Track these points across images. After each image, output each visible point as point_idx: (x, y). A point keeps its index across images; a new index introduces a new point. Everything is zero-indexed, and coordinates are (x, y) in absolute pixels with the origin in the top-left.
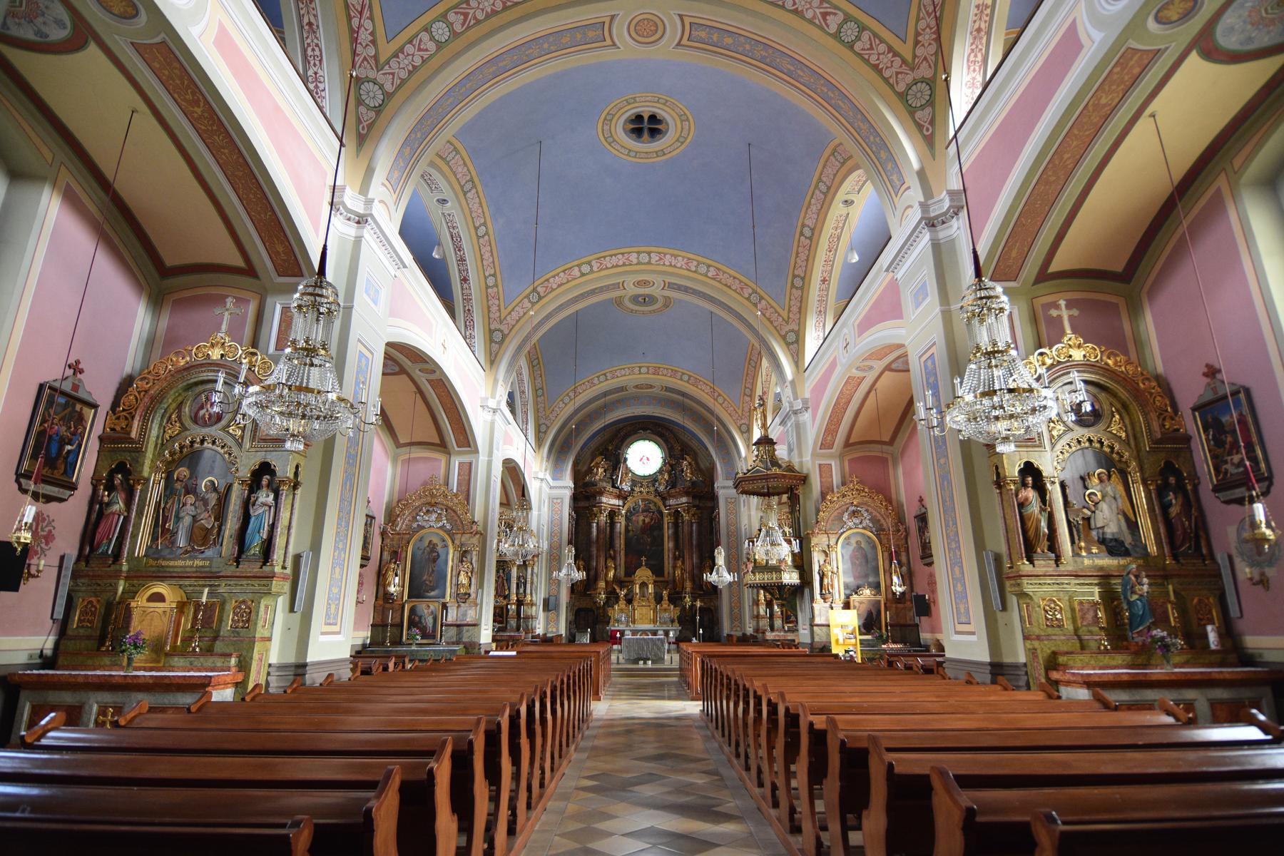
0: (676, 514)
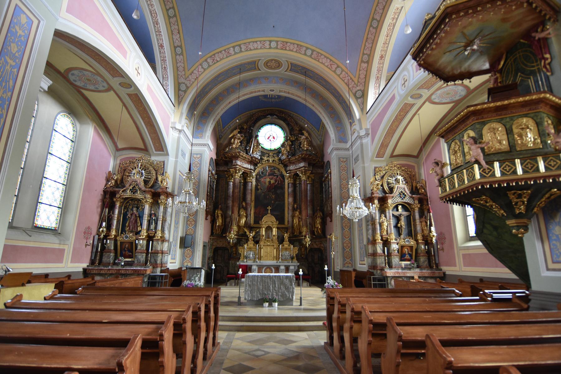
0: (296, 176)
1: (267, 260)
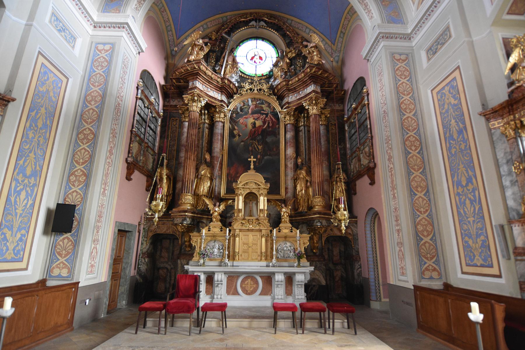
1: (247, 260)
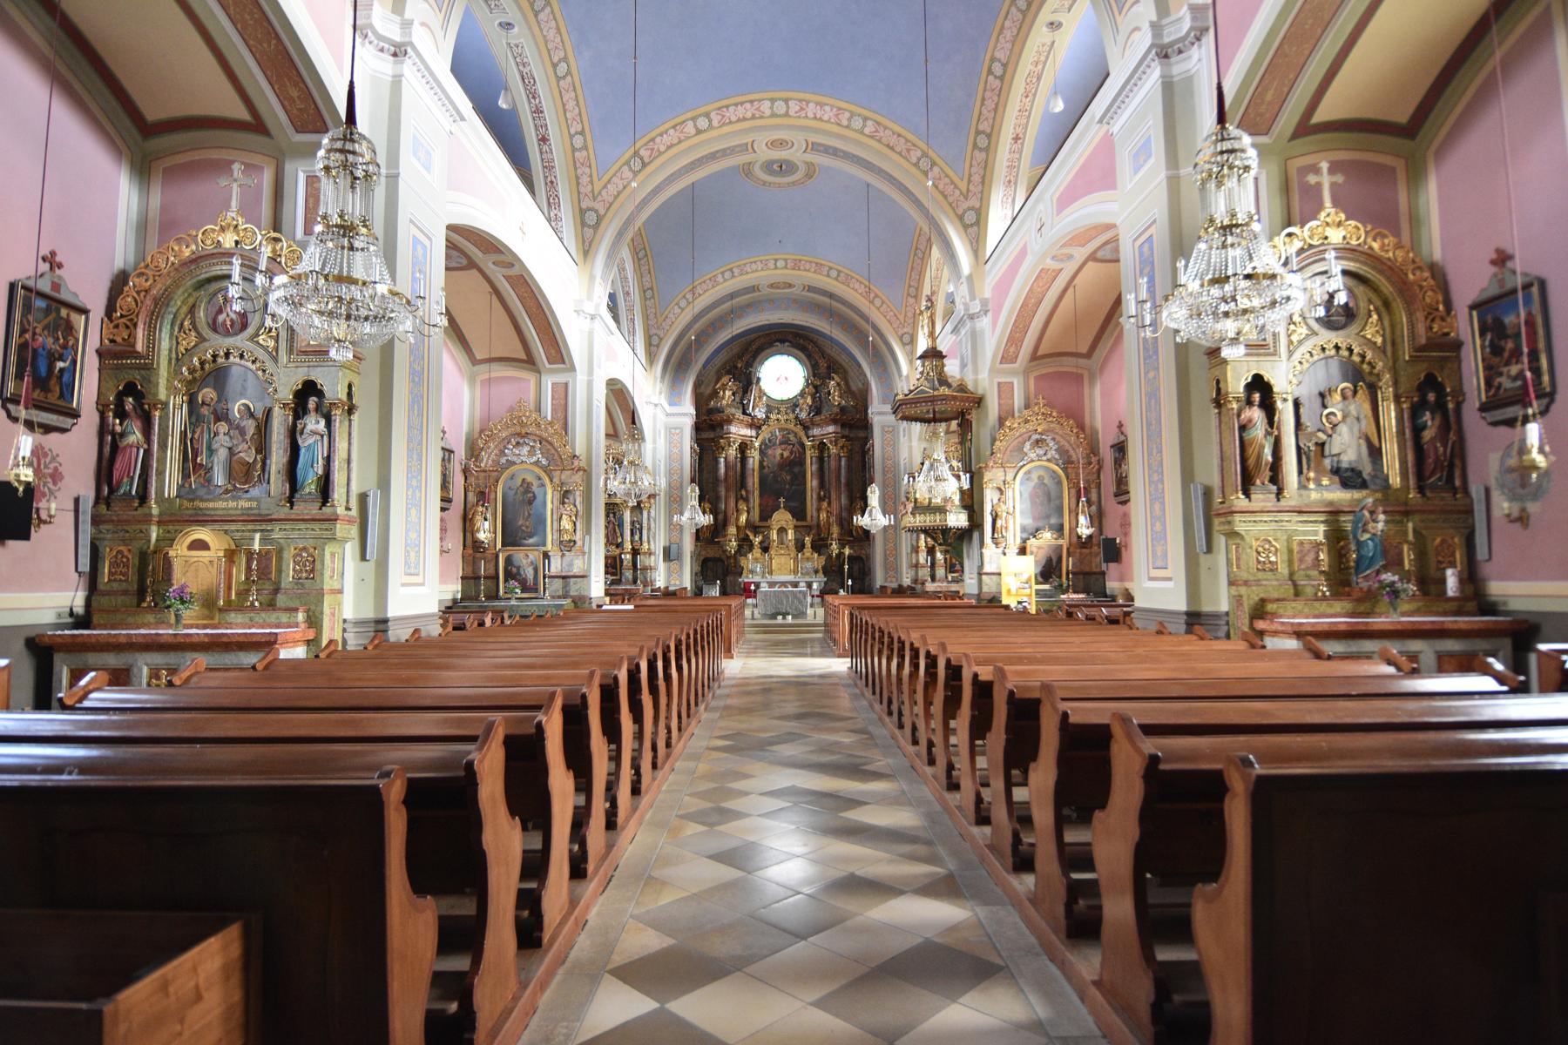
0: (822, 447)
